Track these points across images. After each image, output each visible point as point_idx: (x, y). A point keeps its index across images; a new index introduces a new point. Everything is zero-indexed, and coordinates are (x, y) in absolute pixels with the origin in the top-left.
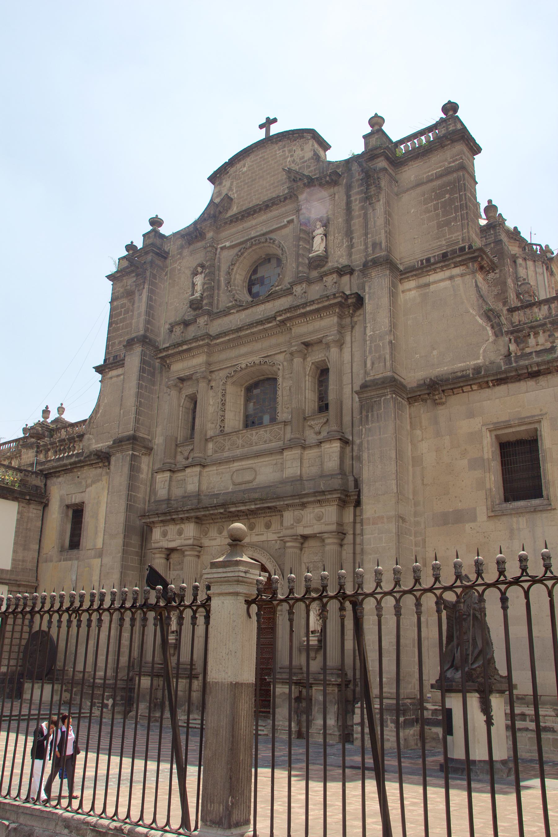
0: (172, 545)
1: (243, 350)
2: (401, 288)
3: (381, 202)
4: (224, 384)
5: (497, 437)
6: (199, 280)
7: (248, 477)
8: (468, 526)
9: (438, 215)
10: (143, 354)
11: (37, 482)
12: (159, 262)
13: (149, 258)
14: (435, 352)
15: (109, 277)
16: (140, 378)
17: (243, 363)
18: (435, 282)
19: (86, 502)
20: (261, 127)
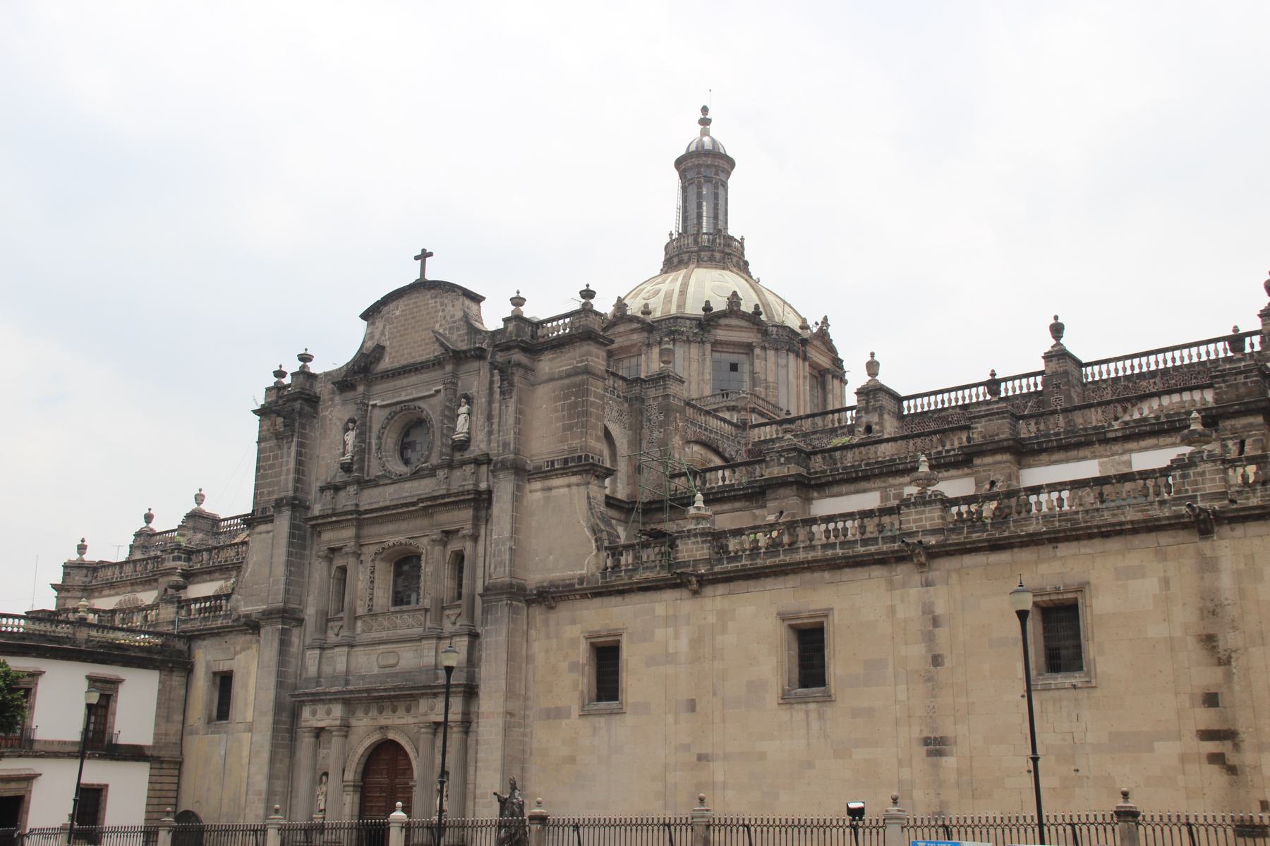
1: (391, 527)
2: (528, 487)
3: (513, 400)
4: (373, 560)
5: (592, 644)
6: (350, 437)
7: (392, 661)
9: (564, 417)
10: (293, 518)
11: (180, 645)
12: (307, 409)
13: (297, 405)
14: (551, 557)
15: (255, 412)
16: (290, 545)
17: (392, 540)
18: (557, 487)
19: (235, 671)
20: (417, 258)
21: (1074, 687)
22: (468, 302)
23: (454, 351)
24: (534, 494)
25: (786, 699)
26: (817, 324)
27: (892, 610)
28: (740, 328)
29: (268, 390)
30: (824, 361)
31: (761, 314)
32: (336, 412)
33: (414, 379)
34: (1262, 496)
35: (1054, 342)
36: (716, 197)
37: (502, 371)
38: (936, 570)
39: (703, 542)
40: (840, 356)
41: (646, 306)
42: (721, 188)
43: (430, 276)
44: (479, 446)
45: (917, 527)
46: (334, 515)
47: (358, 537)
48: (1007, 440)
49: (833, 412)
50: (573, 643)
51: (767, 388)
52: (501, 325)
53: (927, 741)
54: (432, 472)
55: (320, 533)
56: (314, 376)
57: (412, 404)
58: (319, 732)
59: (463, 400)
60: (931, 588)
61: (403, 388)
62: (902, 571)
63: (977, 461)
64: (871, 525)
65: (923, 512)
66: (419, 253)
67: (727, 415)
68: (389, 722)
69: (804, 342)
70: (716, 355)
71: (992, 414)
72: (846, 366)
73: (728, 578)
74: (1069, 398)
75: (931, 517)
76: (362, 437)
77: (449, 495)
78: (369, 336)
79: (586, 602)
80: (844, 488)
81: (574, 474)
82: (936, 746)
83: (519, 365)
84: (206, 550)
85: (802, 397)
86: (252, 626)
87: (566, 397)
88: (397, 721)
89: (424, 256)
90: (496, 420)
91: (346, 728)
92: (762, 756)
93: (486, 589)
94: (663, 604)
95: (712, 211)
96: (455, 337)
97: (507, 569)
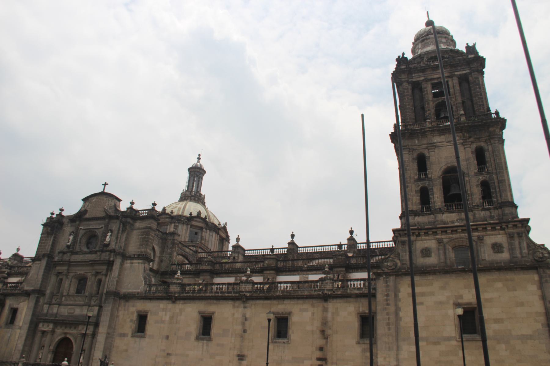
0: (45, 329)
1: (79, 268)
2: (126, 262)
4: (72, 278)
6: (71, 238)
7: (72, 312)
8: (126, 338)
13: (56, 224)
14: (130, 285)
17: (79, 272)
19: (19, 308)
20: (103, 185)
21: (284, 343)
22: (116, 201)
23: (109, 215)
24: (127, 264)
25: (197, 339)
26: (223, 224)
27: (233, 314)
28: (200, 222)
29: (48, 218)
30: (224, 236)
31: (207, 218)
32: (68, 229)
33: (95, 222)
34: (342, 291)
35: (291, 239)
36: (199, 181)
37: (123, 224)
38: (248, 303)
39: (178, 286)
40: (229, 235)
41: (172, 211)
42: (201, 179)
43: (106, 191)
44: (113, 246)
45: (244, 290)
46: (62, 261)
47: (68, 270)
48: (274, 267)
49: (224, 251)
50: (132, 313)
51: (205, 241)
52: (126, 210)
53: (238, 356)
54: (96, 252)
55: (56, 267)
56: (63, 216)
57: (93, 230)
58: (44, 332)
59: (110, 231)
60: (246, 309)
61: (91, 224)
62: (237, 303)
63: (265, 272)
64: (230, 288)
65: (246, 286)
66: (104, 183)
67: (192, 248)
68: (68, 331)
69: (219, 229)
70: (192, 229)
71: (271, 259)
72: (230, 238)
73: (184, 299)
74: (294, 257)
75: (249, 287)
76: (75, 238)
77: (100, 261)
78: (83, 206)
79: (139, 301)
80: (224, 275)
81: (141, 259)
83: (129, 223)
84: (17, 267)
85: (216, 246)
86: (27, 294)
87: (142, 235)
88: (71, 332)
89: (105, 184)
90: (119, 239)
91: (53, 332)
93: (107, 292)
94: (162, 304)
95: (197, 185)
96: (110, 211)
97: (115, 287)
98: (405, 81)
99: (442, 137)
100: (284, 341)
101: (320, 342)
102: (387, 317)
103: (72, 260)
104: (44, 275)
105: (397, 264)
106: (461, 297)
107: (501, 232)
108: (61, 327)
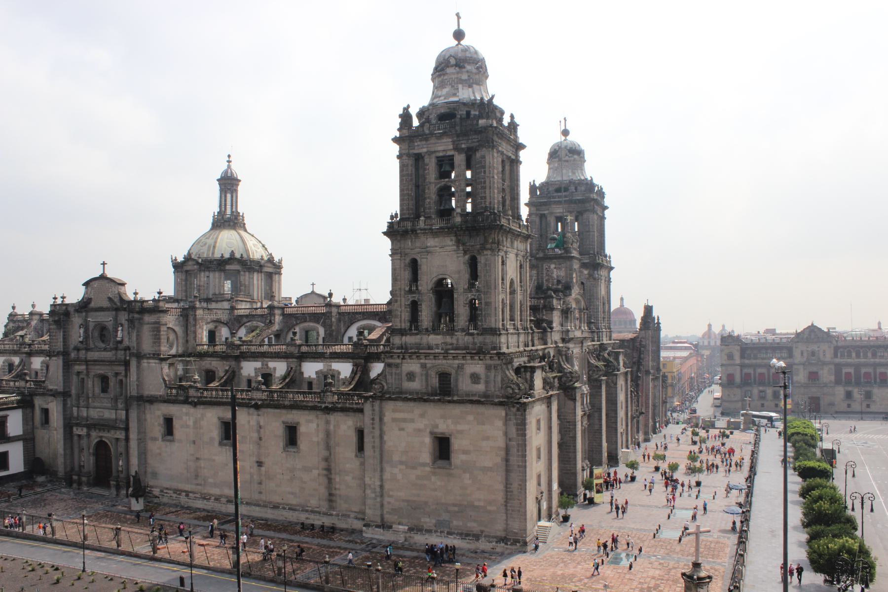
0: (80, 433)
6: (82, 331)
7: (102, 415)
21: (294, 452)
27: (249, 422)
29: (51, 305)
32: (77, 320)
33: (102, 313)
44: (126, 343)
51: (245, 287)
53: (257, 462)
68: (103, 435)
76: (86, 332)
78: (86, 293)
79: (162, 404)
82: (260, 464)
85: (260, 288)
88: (105, 435)
89: (104, 264)
91: (88, 435)
92: (214, 460)
94: (185, 408)
98: (404, 154)
99: (436, 240)
100: (295, 450)
101: (325, 453)
102: (373, 440)
103: (89, 358)
104: (64, 376)
105: (383, 386)
106: (437, 426)
107: (480, 362)
108: (95, 431)
